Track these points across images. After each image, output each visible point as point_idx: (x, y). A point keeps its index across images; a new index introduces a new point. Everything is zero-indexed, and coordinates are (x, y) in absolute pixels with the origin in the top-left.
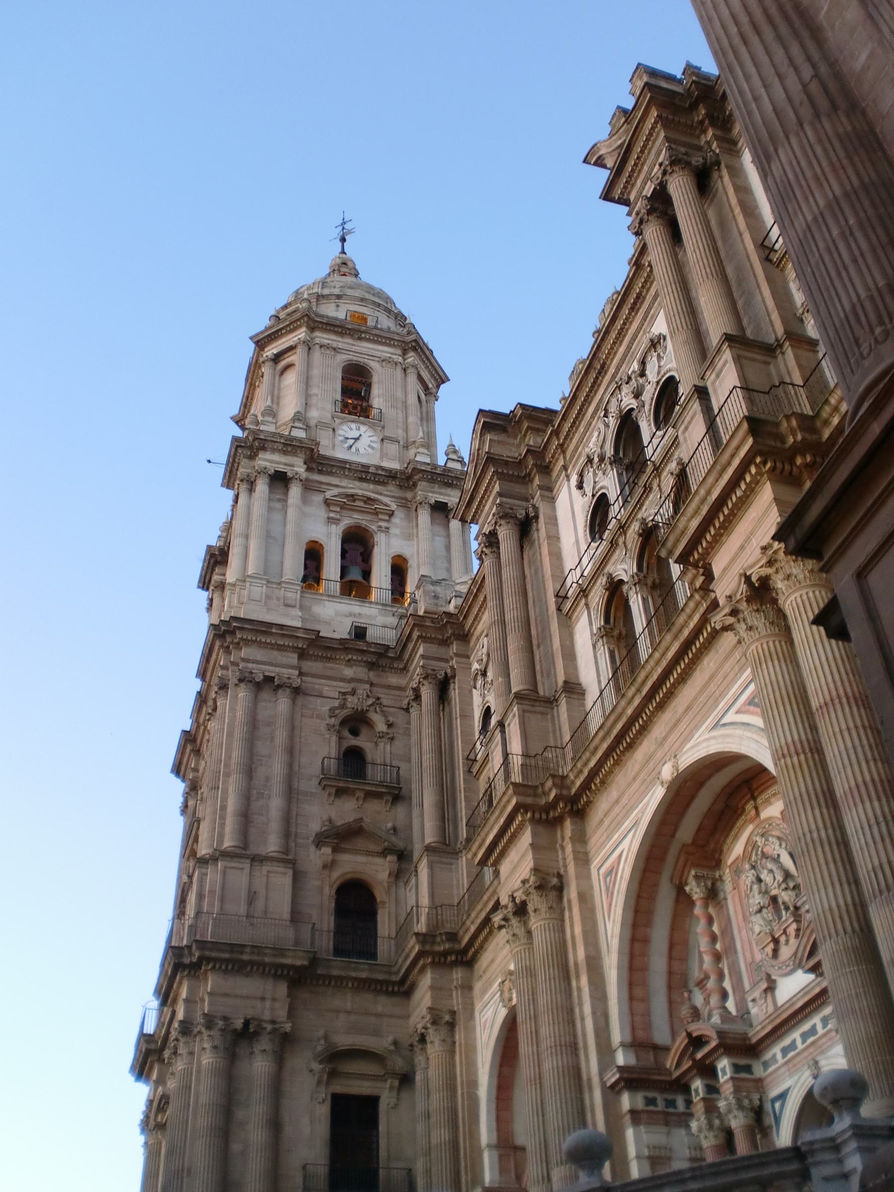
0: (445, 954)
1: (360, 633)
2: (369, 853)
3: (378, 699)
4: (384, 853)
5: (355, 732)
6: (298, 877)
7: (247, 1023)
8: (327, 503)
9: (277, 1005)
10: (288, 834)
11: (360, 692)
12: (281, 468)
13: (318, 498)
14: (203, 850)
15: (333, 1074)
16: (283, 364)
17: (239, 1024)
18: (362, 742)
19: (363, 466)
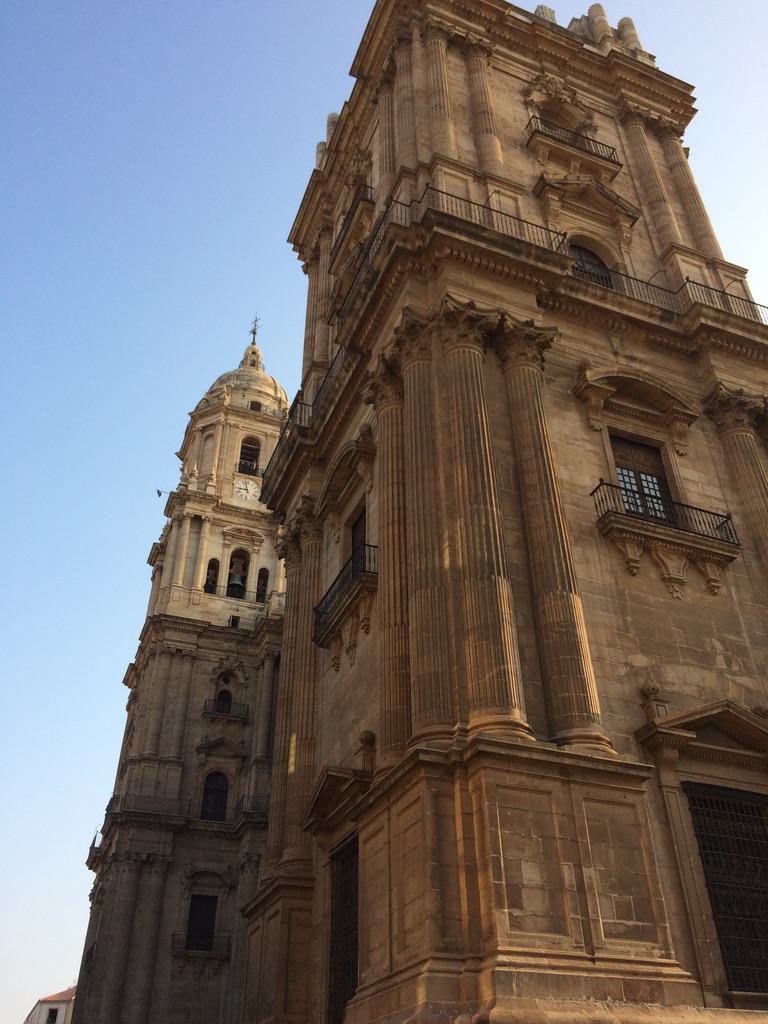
0: (259, 823)
1: (235, 621)
2: (226, 757)
3: (241, 662)
4: (236, 757)
5: (227, 681)
6: (185, 771)
7: (149, 855)
8: (224, 534)
9: (167, 846)
10: (181, 746)
11: (231, 659)
12: (198, 513)
13: (219, 530)
14: (133, 754)
15: (194, 884)
16: (207, 433)
17: (144, 857)
18: (230, 687)
19: (248, 510)
